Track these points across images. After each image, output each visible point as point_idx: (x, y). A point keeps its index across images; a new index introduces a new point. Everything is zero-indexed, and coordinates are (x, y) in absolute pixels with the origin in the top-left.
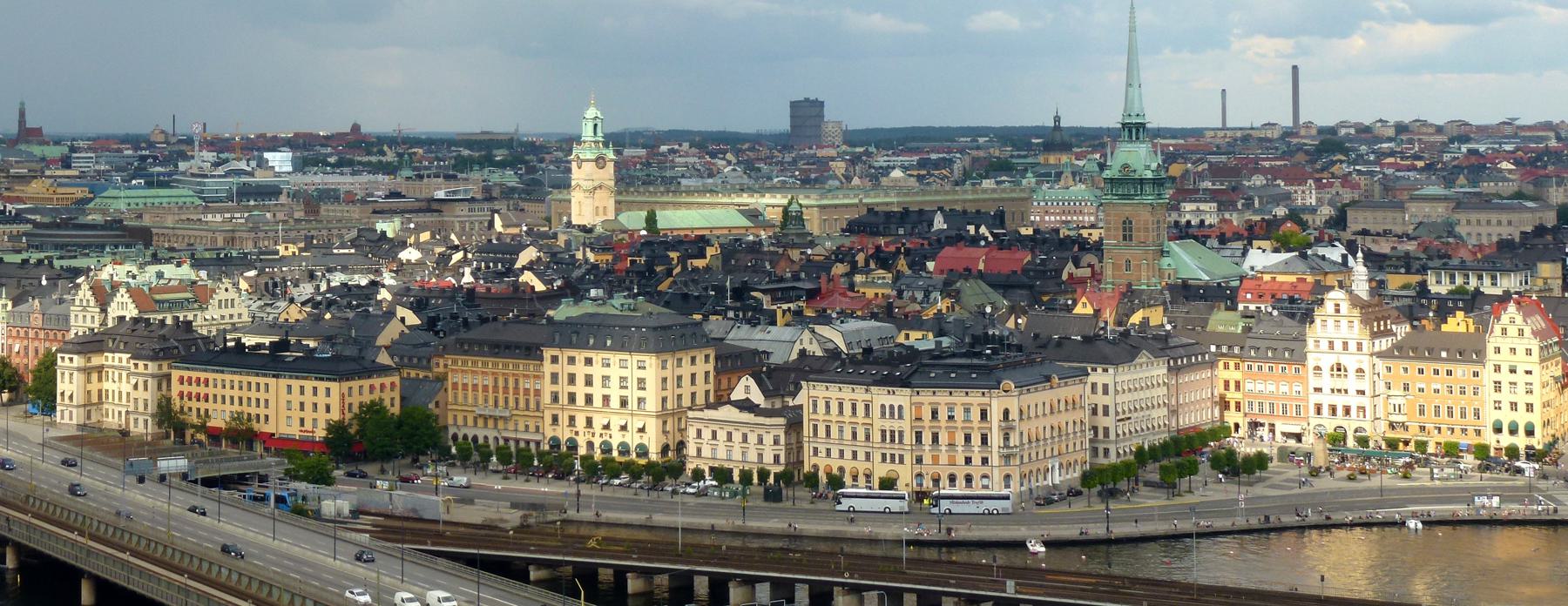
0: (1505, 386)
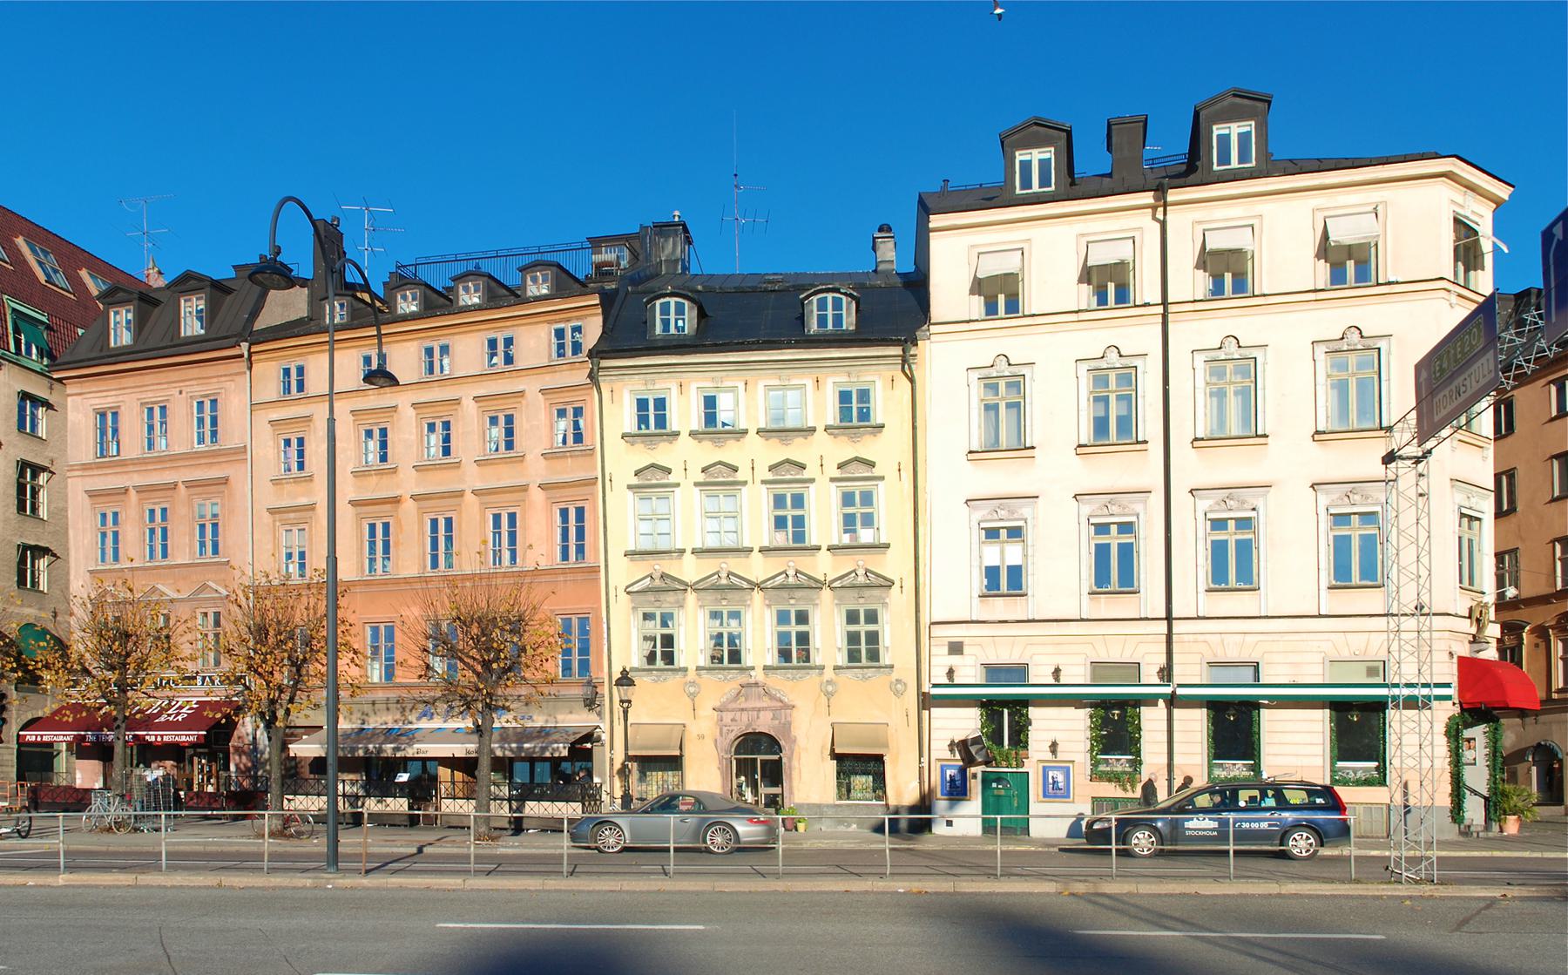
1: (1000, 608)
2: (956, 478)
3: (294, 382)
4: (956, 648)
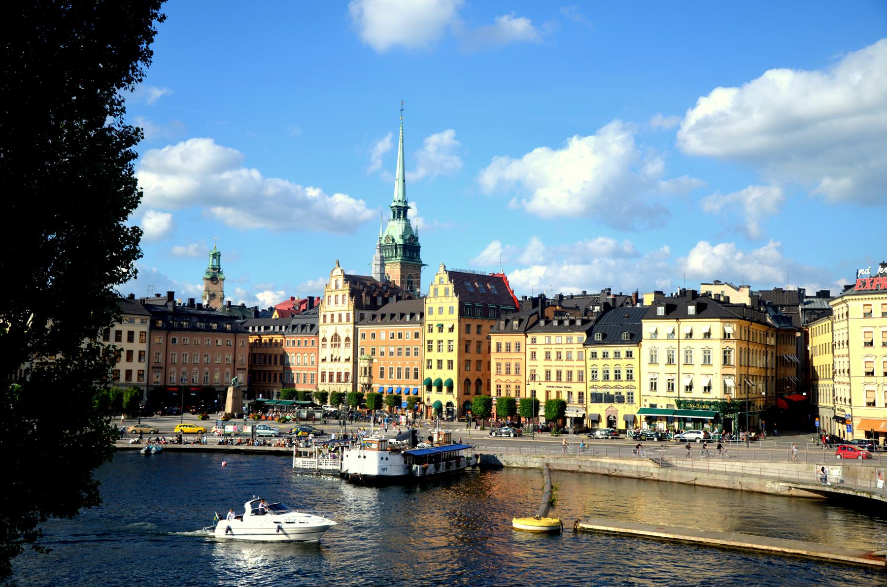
3: (534, 341)
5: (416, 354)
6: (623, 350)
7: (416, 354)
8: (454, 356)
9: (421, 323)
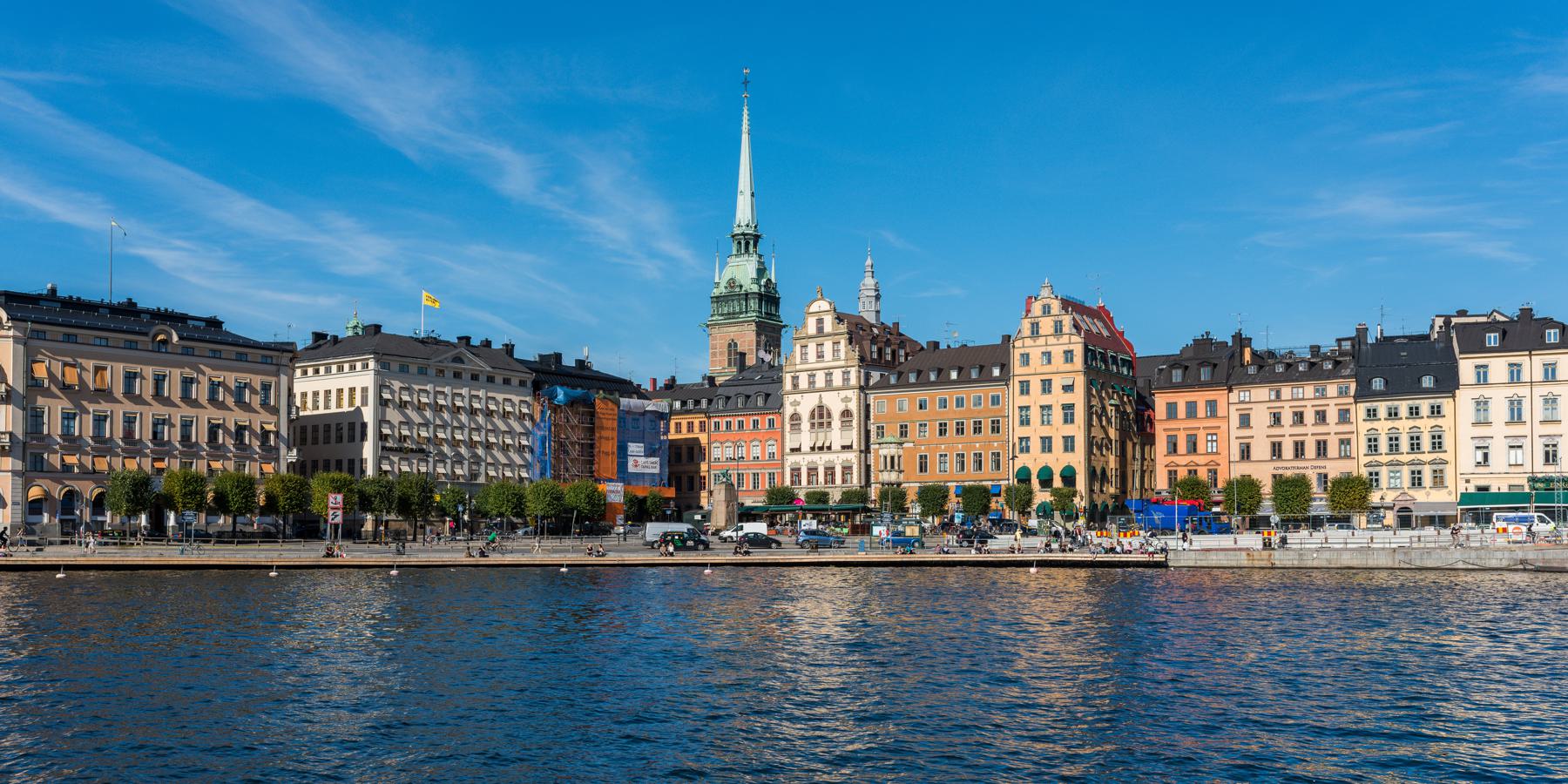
0: (1035, 414)
1: (1481, 470)
2: (1466, 431)
4: (1468, 481)
5: (996, 429)
6: (1425, 406)
7: (996, 429)
8: (1078, 431)
9: (1005, 378)
